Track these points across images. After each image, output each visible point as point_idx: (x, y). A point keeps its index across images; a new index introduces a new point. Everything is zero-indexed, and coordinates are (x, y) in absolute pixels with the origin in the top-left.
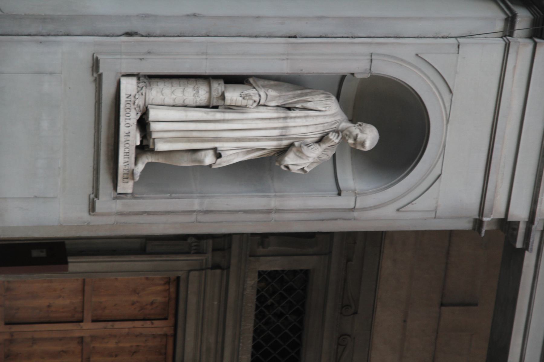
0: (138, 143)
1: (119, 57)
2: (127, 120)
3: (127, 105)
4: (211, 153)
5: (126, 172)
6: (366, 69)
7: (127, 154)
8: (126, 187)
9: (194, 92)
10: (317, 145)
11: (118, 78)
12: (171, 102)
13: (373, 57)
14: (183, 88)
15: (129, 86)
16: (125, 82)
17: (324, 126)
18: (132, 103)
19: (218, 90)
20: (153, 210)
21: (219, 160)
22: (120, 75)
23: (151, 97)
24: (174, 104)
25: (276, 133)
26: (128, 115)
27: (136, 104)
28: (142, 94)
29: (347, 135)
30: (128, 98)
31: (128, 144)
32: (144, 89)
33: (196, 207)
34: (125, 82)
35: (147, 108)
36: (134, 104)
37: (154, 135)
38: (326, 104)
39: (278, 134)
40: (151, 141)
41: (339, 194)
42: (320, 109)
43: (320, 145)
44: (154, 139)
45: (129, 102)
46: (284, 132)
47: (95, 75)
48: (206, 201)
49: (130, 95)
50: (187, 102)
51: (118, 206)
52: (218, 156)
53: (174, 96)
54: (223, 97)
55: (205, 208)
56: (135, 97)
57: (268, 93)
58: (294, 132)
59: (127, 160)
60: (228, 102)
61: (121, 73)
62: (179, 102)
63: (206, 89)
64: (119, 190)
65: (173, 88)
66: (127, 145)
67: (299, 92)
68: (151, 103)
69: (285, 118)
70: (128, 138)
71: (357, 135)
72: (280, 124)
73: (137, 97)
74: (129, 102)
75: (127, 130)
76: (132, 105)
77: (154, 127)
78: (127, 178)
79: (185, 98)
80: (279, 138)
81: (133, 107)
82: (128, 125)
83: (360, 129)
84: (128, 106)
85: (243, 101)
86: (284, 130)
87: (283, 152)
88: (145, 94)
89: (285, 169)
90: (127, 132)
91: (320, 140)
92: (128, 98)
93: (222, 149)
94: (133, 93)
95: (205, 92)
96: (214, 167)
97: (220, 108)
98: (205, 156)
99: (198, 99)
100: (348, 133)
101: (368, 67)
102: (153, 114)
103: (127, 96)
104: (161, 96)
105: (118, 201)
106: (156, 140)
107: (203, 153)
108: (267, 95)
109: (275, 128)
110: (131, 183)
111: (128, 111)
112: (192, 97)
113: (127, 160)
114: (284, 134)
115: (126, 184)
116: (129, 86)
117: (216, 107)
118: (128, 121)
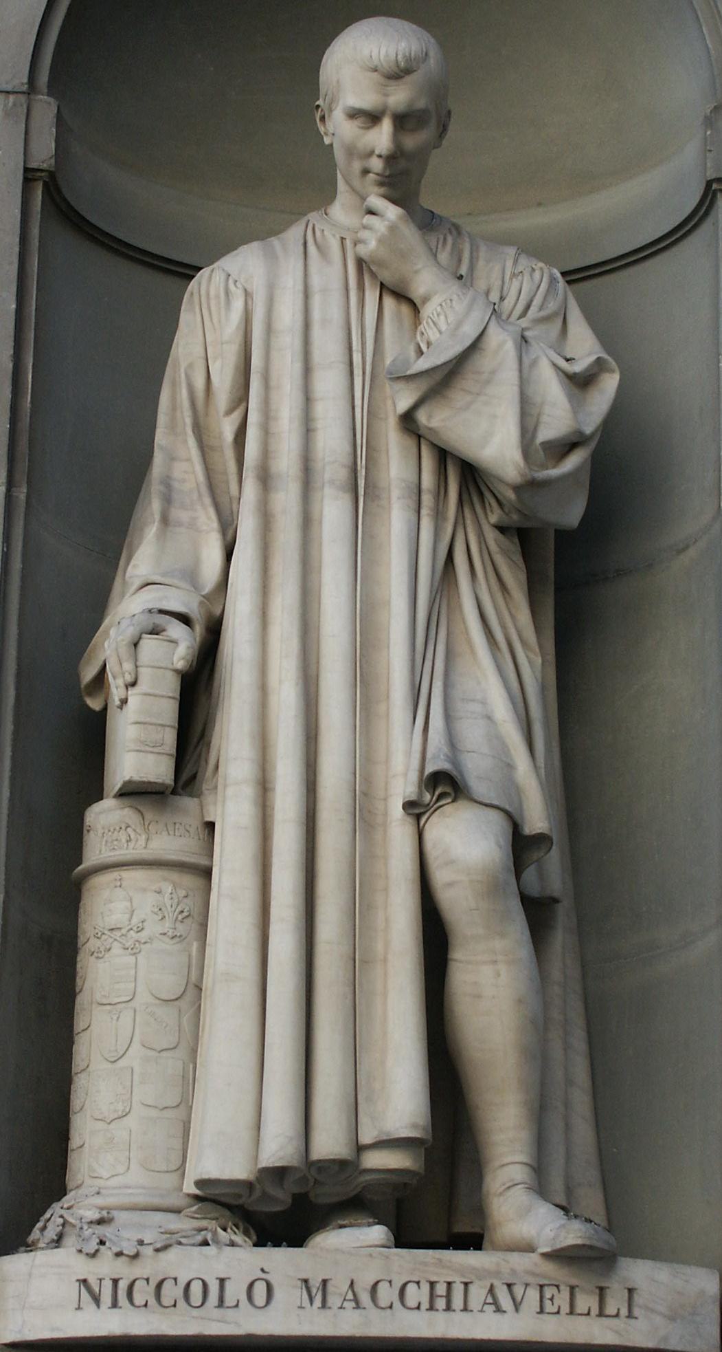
0: (378, 1233)
2: (230, 1300)
3: (139, 1299)
5: (563, 1300)
7: (441, 1297)
10: (428, 311)
12: (173, 1064)
14: (97, 1010)
17: (324, 291)
18: (125, 1271)
21: (478, 787)
24: (182, 1053)
25: (333, 512)
26: (196, 1288)
28: (101, 1222)
29: (366, 172)
35: (197, 1198)
37: (329, 1143)
38: (217, 297)
39: (345, 501)
43: (426, 300)
45: (123, 1285)
50: (171, 983)
57: (137, 583)
59: (478, 1294)
60: (159, 769)
63: (106, 894)
66: (387, 1294)
68: (170, 1181)
69: (265, 479)
70: (339, 1287)
71: (354, 114)
72: (287, 499)
74: (123, 1285)
77: (278, 1147)
78: (602, 1291)
79: (143, 997)
80: (362, 487)
82: (260, 1289)
83: (331, 110)
85: (143, 686)
86: (327, 476)
89: (574, 460)
90: (299, 1295)
92: (97, 1300)
93: (414, 776)
96: (537, 819)
97: (208, 819)
98: (451, 862)
99: (153, 928)
100: (357, 166)
102: (222, 1158)
103: (85, 1295)
104: (131, 1122)
106: (366, 1138)
107: (440, 877)
110: (637, 1272)
111: (171, 1292)
112: (140, 957)
113: (478, 1294)
114: (343, 474)
117: (211, 826)
118: (235, 1291)
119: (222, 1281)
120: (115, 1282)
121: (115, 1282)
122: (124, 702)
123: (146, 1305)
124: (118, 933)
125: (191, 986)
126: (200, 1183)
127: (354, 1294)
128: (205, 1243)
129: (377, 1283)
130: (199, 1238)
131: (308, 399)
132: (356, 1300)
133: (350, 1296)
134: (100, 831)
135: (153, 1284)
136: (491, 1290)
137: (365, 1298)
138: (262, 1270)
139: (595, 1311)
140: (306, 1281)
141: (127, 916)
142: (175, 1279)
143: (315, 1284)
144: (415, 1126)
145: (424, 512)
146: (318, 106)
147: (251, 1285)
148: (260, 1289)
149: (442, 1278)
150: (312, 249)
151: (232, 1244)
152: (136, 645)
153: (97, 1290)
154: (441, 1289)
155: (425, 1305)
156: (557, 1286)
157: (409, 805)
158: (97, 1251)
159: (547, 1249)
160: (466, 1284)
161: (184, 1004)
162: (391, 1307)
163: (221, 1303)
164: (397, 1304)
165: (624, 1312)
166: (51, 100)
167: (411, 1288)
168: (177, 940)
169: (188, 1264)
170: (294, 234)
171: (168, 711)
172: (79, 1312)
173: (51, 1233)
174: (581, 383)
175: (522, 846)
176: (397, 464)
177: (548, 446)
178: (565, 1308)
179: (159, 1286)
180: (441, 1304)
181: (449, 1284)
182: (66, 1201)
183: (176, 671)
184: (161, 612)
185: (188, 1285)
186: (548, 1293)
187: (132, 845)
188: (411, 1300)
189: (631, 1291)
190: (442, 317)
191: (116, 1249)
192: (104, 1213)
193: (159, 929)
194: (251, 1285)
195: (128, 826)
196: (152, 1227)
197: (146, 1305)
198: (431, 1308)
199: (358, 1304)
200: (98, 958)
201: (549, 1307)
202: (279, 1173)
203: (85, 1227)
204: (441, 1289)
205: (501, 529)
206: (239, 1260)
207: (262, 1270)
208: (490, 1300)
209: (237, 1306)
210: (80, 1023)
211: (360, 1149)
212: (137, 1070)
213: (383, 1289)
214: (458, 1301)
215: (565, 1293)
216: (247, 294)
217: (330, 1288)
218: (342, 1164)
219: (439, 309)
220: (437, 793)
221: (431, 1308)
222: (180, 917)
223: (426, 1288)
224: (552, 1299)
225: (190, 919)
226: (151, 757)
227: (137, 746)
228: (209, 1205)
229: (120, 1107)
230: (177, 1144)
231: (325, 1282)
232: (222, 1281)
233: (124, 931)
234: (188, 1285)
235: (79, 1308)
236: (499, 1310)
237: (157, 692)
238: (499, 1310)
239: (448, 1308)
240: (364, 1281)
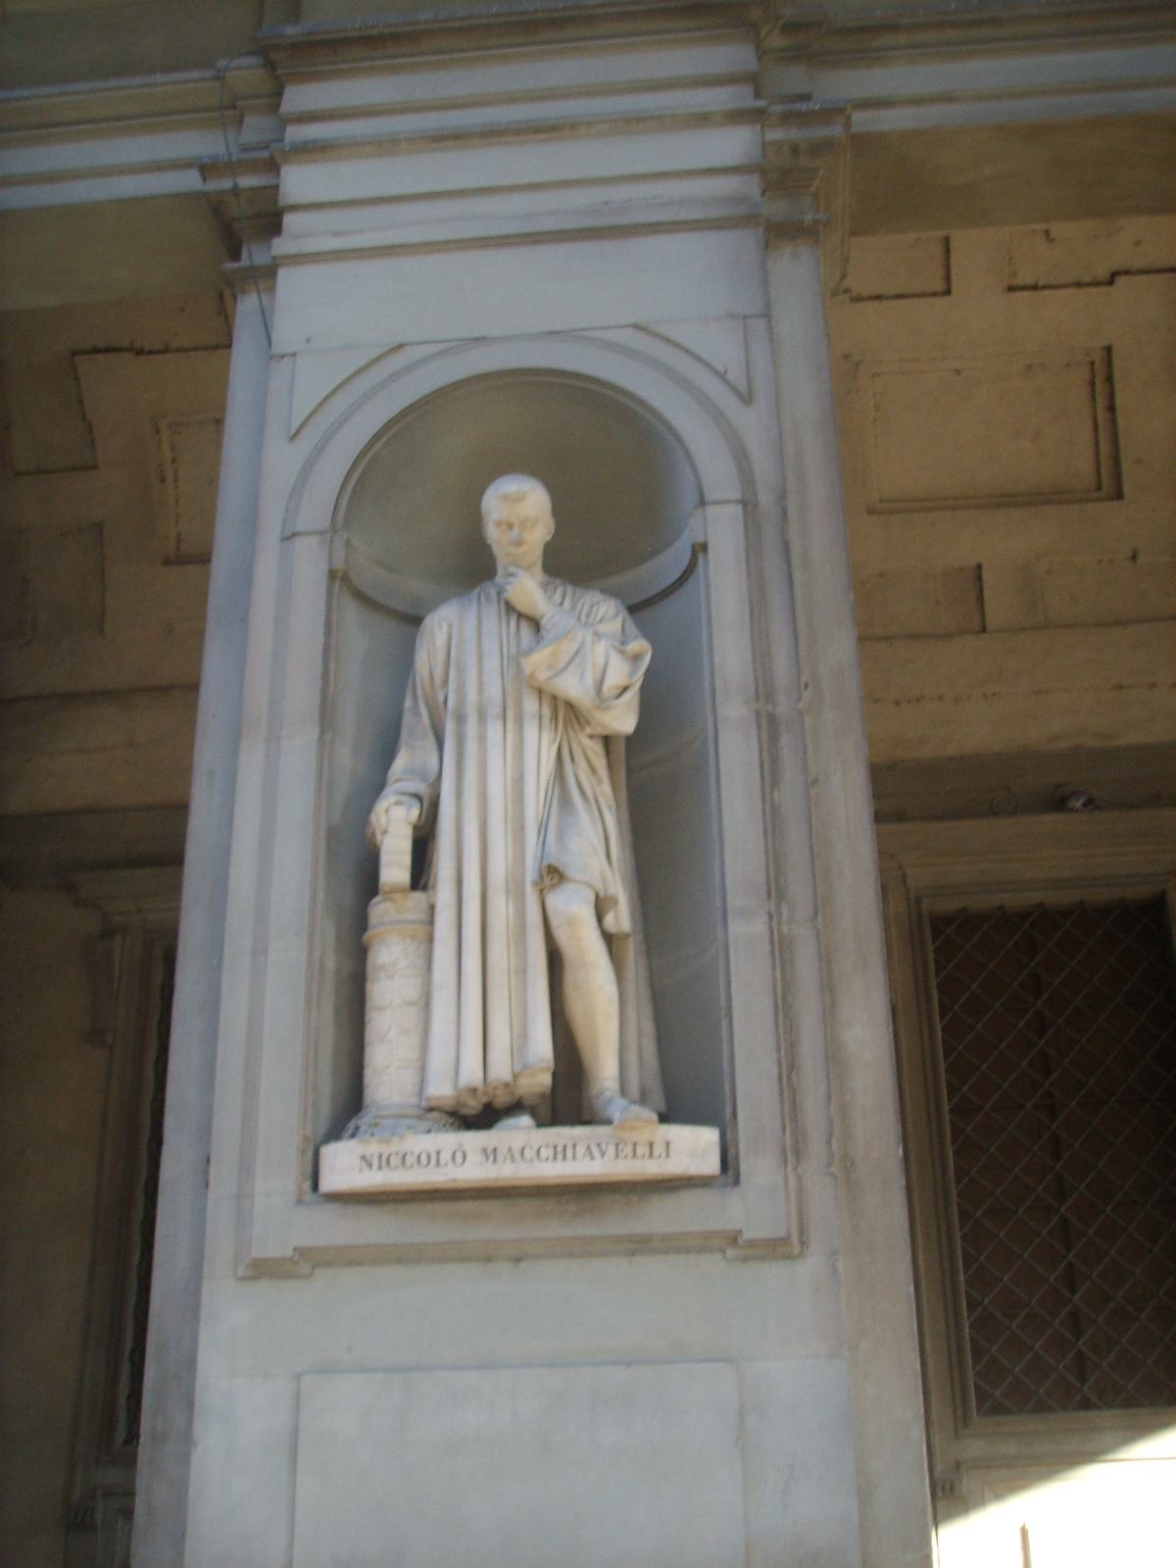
4: (554, 901)
5: (629, 1150)
7: (560, 1153)
10: (543, 622)
12: (414, 1039)
13: (288, 533)
16: (330, 1182)
25: (494, 731)
26: (424, 1158)
30: (370, 1166)
33: (759, 926)
34: (330, 1182)
35: (431, 1109)
41: (704, 547)
42: (441, 640)
45: (384, 1157)
47: (305, 1269)
48: (734, 901)
49: (363, 1158)
51: (760, 1168)
52: (553, 875)
57: (393, 780)
58: (494, 691)
61: (301, 1192)
62: (412, 1015)
67: (408, 704)
70: (502, 1150)
71: (498, 524)
74: (384, 1157)
75: (474, 1158)
78: (651, 1145)
81: (396, 1146)
84: (394, 1161)
88: (375, 1117)
92: (370, 1166)
101: (314, 540)
109: (482, 738)
111: (410, 1160)
113: (581, 1150)
115: (672, 1148)
116: (346, 1165)
118: (445, 1157)
119: (438, 1153)
121: (380, 1156)
128: (429, 1131)
129: (523, 1149)
131: (480, 673)
132: (512, 1157)
135: (400, 1156)
136: (588, 1148)
137: (517, 1156)
139: (647, 1154)
150: (483, 599)
154: (560, 1149)
157: (535, 884)
163: (438, 1163)
164: (535, 1159)
165: (664, 1155)
170: (477, 591)
173: (350, 1132)
176: (531, 705)
178: (630, 1155)
180: (560, 1156)
185: (419, 1156)
186: (620, 1147)
189: (668, 1144)
199: (513, 1159)
202: (474, 1091)
204: (560, 1149)
205: (591, 737)
210: (367, 1018)
213: (527, 1152)
216: (450, 626)
218: (507, 1085)
221: (555, 1158)
224: (623, 1150)
227: (395, 868)
231: (495, 1150)
234: (419, 1156)
236: (592, 1158)
238: (592, 1158)
239: (564, 1158)
240: (517, 1146)
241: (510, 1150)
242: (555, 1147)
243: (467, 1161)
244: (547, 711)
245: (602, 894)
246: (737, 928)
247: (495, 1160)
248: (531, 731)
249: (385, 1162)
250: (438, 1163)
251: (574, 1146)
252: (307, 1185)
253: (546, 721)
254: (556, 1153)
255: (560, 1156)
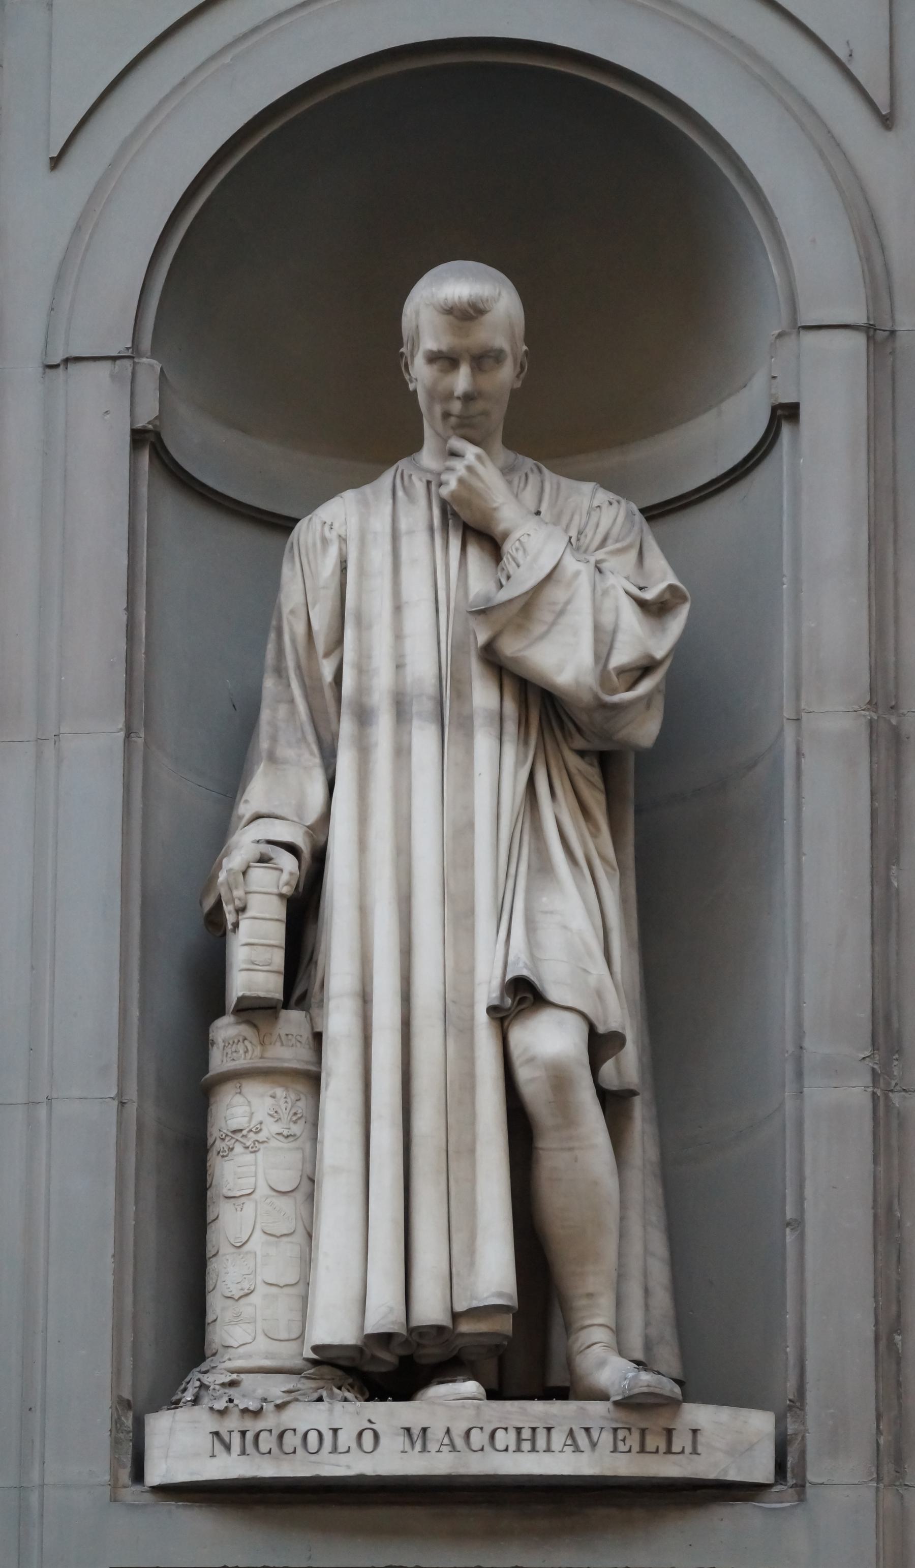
1: (34, 1498)
2: (342, 1447)
3: (264, 1447)
6: (113, 377)
7: (527, 1439)
8: (727, 1439)
9: (238, 1148)
10: (509, 547)
11: (149, 1498)
12: (290, 1249)
15: (182, 1447)
18: (253, 1426)
19: (227, 1043)
20: (870, 1302)
21: (553, 993)
22: (131, 1493)
23: (262, 1344)
26: (313, 1438)
27: (253, 1405)
30: (228, 1447)
31: (468, 1433)
32: (207, 1379)
35: (315, 1363)
36: (257, 1414)
40: (465, 1327)
43: (506, 535)
44: (456, 1316)
46: (422, 706)
50: (287, 1179)
53: (257, 1242)
54: (255, 1011)
55: (853, 1049)
56: (222, 1413)
59: (558, 1438)
64: (760, 1469)
65: (225, 1249)
66: (477, 1438)
70: (437, 1433)
73: (221, 1405)
74: (249, 1436)
75: (392, 1443)
76: (260, 1424)
79: (263, 1190)
81: (270, 1420)
82: (368, 1438)
84: (266, 1442)
86: (415, 708)
87: (541, 710)
89: (645, 686)
90: (401, 1441)
91: (480, 534)
92: (228, 1447)
94: (210, 1423)
95: (238, 1099)
97: (319, 1030)
99: (271, 1128)
101: (103, 370)
102: (334, 1328)
103: (218, 1446)
105: (811, 1477)
106: (460, 1307)
107: (523, 1074)
108: (258, 817)
109: (402, 752)
111: (291, 1441)
112: (259, 1155)
113: (558, 1438)
116: (182, 1447)
117: (318, 1037)
118: (346, 1439)
119: (335, 1431)
120: (243, 1433)
121: (243, 1433)
122: (236, 925)
123: (270, 1452)
124: (238, 1136)
125: (305, 1180)
126: (316, 1349)
127: (451, 1440)
128: (320, 1399)
130: (316, 1396)
131: (398, 636)
133: (446, 1441)
134: (221, 1045)
135: (275, 1433)
136: (571, 1433)
137: (459, 1442)
138: (370, 1421)
140: (408, 1430)
141: (247, 1119)
142: (294, 1430)
143: (416, 1432)
144: (500, 1295)
145: (506, 738)
146: (402, 354)
147: (360, 1434)
148: (368, 1438)
149: (526, 1425)
151: (346, 1400)
152: (244, 873)
153: (227, 1439)
154: (526, 1434)
155: (512, 1447)
156: (629, 1429)
158: (226, 1408)
159: (619, 1398)
160: (549, 1429)
161: (300, 1196)
162: (482, 1450)
163: (335, 1449)
164: (488, 1448)
166: (154, 362)
167: (500, 1434)
168: (291, 1139)
169: (309, 1417)
171: (277, 933)
172: (214, 1459)
174: (655, 610)
175: (600, 1045)
176: (484, 695)
177: (621, 671)
179: (281, 1436)
180: (526, 1446)
181: (534, 1429)
182: (204, 1367)
183: (281, 896)
184: (270, 842)
186: (621, 1434)
187: (249, 1055)
188: (500, 1445)
190: (521, 552)
191: (241, 1407)
192: (234, 1376)
193: (276, 1128)
194: (360, 1434)
195: (245, 1039)
196: (276, 1387)
197: (270, 1452)
198: (519, 1449)
199: (453, 1448)
200: (223, 1156)
201: (621, 1447)
202: (385, 1339)
203: (217, 1387)
204: (526, 1434)
206: (348, 1414)
207: (370, 1421)
208: (569, 1442)
209: (348, 1451)
211: (456, 1316)
212: (259, 1253)
214: (541, 1443)
215: (636, 1435)
217: (429, 1433)
219: (517, 543)
220: (518, 998)
221: (519, 1449)
222: (294, 1118)
223: (512, 1434)
225: (302, 1121)
226: (261, 974)
228: (325, 1369)
229: (246, 1286)
230: (297, 1316)
231: (424, 1430)
232: (335, 1431)
233: (244, 1132)
234: (305, 1435)
235: (213, 1456)
236: (577, 1449)
237: (267, 916)
239: (533, 1449)
241: (448, 1431)
242: (519, 1430)
243: (379, 1449)
244: (510, 708)
245: (601, 1029)
246: (820, 1095)
247: (424, 1449)
248: (483, 743)
249: (251, 1443)
250: (335, 1449)
251: (549, 1429)
252: (125, 1475)
253: (511, 727)
254: (519, 1440)
255: (526, 1446)
